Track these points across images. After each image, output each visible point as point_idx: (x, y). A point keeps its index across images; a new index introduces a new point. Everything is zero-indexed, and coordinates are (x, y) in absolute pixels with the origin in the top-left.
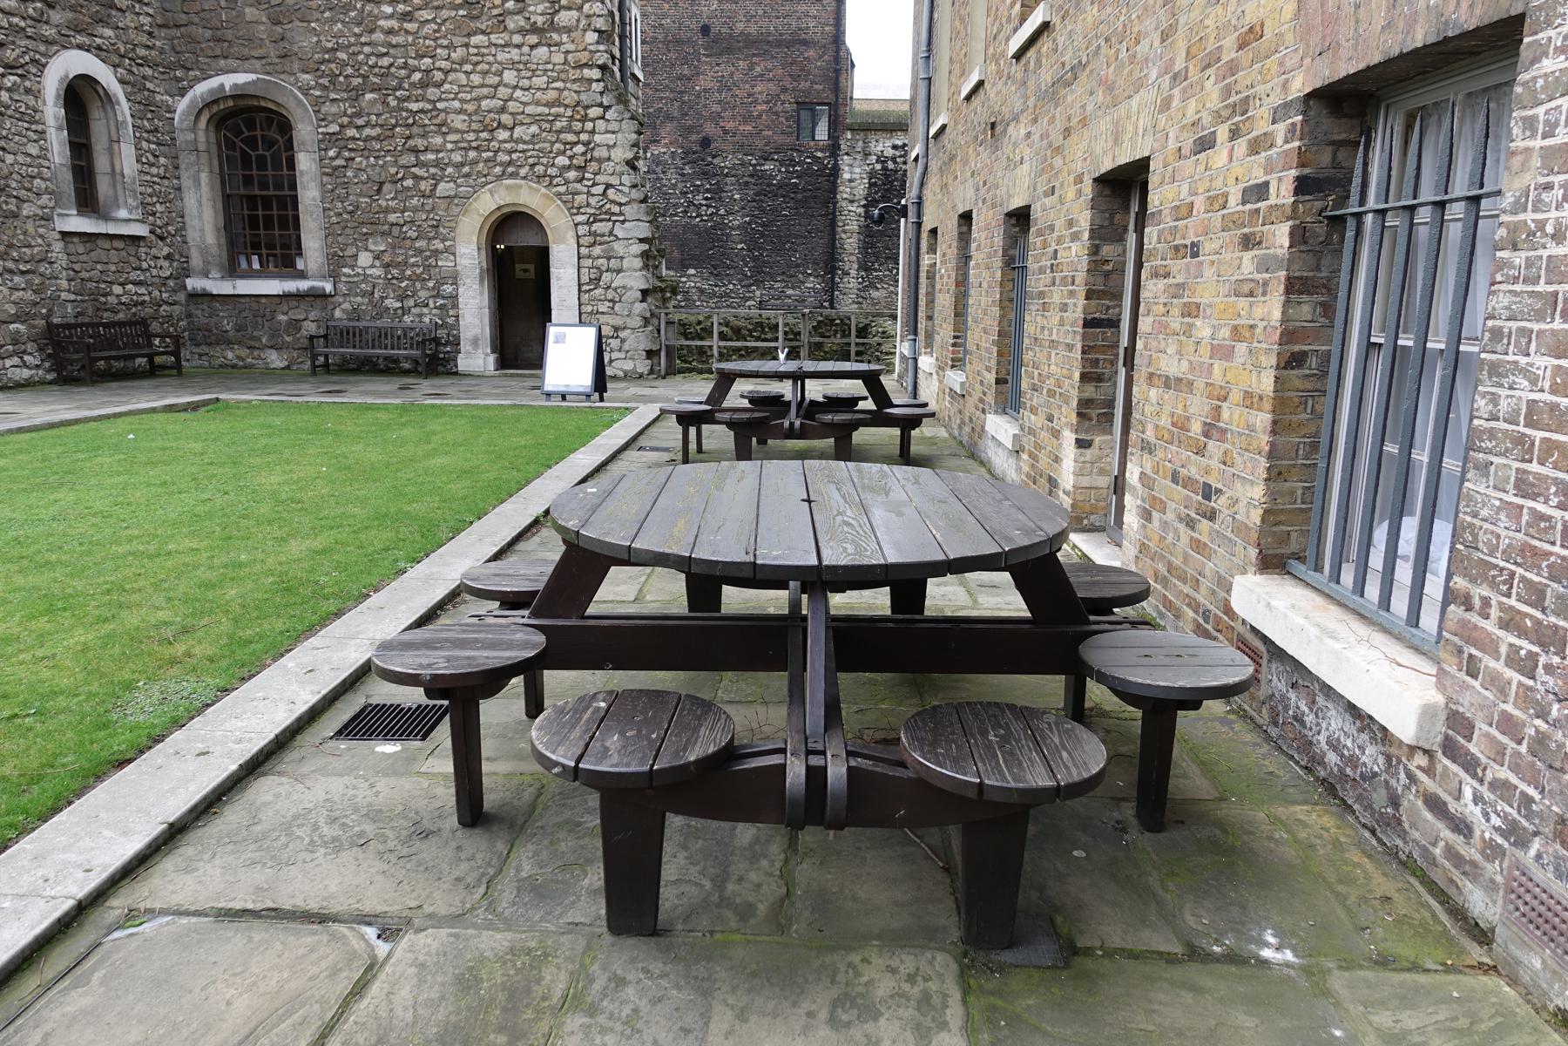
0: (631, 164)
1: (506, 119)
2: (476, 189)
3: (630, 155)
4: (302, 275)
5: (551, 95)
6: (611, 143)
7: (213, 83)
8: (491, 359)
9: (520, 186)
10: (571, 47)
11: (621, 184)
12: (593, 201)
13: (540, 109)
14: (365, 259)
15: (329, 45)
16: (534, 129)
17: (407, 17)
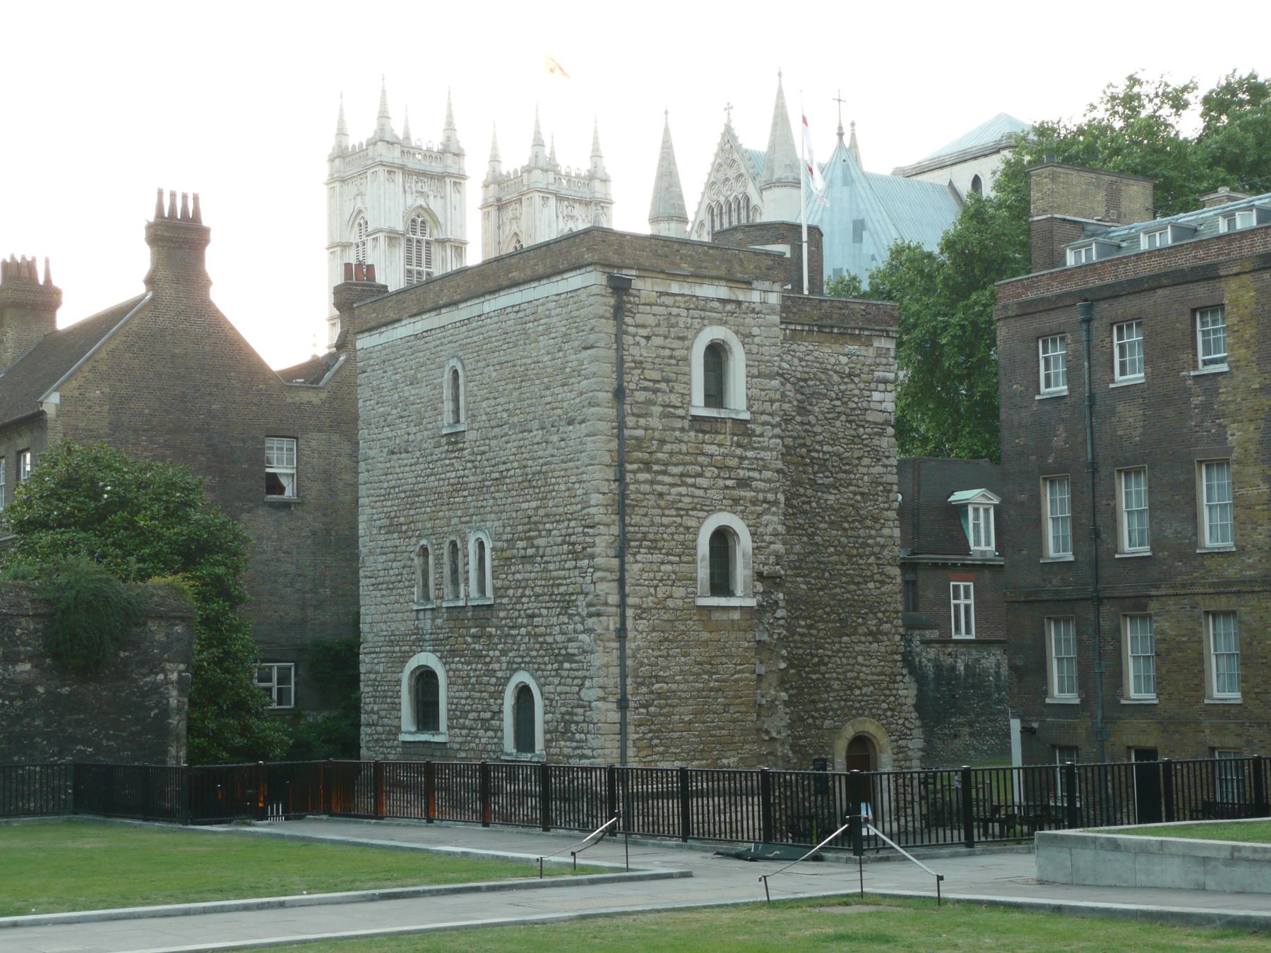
0: (914, 706)
1: (858, 682)
2: (844, 723)
5: (879, 669)
9: (865, 721)
10: (888, 643)
12: (899, 727)
13: (875, 677)
17: (810, 627)
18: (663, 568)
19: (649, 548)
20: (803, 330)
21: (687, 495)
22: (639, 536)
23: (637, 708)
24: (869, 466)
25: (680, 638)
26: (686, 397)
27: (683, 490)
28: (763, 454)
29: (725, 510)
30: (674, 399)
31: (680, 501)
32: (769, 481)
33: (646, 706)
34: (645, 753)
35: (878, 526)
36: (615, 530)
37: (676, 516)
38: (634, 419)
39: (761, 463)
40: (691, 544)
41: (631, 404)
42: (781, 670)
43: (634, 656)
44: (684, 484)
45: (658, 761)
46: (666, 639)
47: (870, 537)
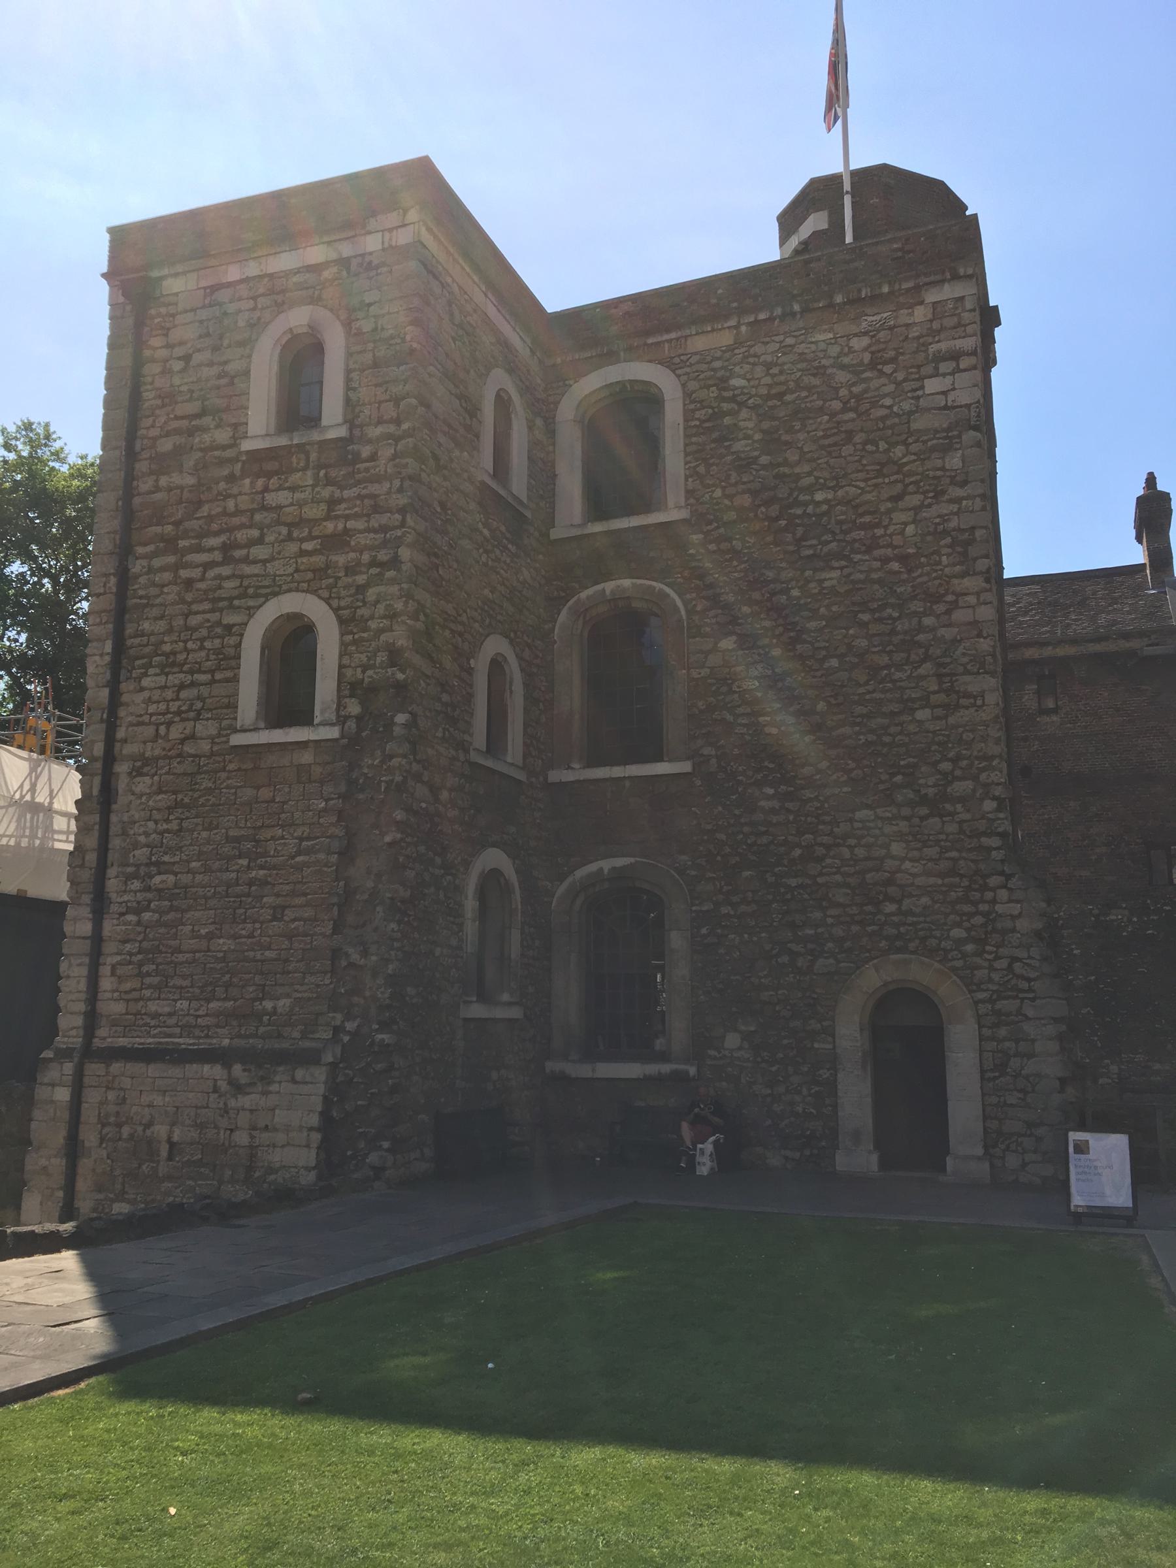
1: (892, 890)
3: (1039, 925)
4: (664, 1057)
6: (1016, 912)
7: (592, 867)
8: (874, 1158)
10: (968, 816)
11: (1030, 957)
12: (996, 977)
13: (932, 880)
14: (732, 1040)
15: (709, 827)
16: (925, 900)
18: (184, 694)
19: (162, 667)
20: (771, 319)
21: (233, 576)
22: (147, 650)
23: (122, 914)
24: (917, 509)
25: (202, 800)
26: (239, 430)
27: (226, 571)
28: (374, 488)
29: (297, 590)
30: (222, 436)
31: (220, 587)
32: (384, 529)
33: (137, 912)
34: (128, 986)
35: (940, 608)
36: (108, 647)
37: (212, 611)
38: (154, 477)
39: (366, 501)
40: (232, 651)
41: (151, 458)
42: (390, 844)
43: (124, 833)
44: (227, 560)
45: (149, 999)
46: (177, 804)
47: (921, 629)
